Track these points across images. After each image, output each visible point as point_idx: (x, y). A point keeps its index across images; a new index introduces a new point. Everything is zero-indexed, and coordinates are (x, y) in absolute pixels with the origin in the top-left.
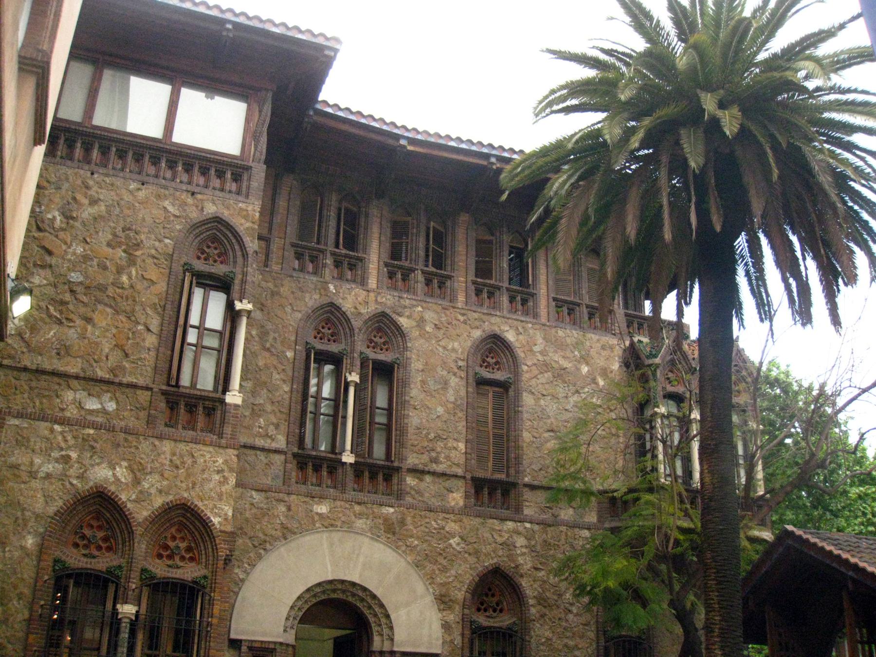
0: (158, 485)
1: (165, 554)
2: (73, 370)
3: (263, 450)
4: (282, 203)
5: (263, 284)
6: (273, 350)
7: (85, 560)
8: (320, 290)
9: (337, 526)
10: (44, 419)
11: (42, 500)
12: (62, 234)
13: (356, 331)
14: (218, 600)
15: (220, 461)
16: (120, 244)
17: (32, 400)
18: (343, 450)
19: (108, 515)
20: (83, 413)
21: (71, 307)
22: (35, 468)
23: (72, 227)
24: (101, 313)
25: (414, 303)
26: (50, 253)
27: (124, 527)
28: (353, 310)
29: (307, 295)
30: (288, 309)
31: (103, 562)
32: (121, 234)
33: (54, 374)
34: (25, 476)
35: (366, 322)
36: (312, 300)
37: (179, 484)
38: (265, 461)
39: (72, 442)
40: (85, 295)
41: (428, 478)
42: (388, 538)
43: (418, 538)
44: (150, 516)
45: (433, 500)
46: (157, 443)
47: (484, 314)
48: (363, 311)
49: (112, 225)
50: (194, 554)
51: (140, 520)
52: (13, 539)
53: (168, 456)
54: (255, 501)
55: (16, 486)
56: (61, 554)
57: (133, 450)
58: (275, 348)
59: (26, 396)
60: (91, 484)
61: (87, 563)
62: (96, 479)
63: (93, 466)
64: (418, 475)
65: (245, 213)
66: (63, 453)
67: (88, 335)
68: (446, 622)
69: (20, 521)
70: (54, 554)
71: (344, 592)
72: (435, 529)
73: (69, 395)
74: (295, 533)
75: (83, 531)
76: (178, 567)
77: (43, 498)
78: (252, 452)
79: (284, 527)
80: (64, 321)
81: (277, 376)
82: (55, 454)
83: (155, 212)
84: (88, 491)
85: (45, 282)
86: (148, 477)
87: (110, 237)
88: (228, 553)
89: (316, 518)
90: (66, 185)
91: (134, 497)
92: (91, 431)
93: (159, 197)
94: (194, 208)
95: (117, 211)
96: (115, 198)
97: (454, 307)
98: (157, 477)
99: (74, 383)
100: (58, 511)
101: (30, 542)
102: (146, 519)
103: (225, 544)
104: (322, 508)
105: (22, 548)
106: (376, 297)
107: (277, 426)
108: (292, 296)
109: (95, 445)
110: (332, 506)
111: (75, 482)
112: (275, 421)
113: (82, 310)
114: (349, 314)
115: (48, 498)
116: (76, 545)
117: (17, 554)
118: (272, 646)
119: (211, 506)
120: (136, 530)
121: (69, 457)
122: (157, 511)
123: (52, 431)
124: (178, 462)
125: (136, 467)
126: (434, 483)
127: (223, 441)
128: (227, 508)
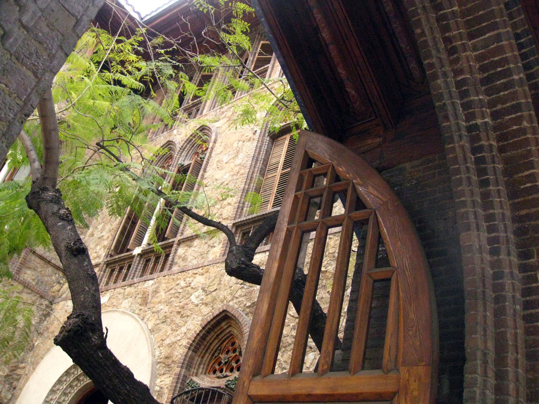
42: (141, 310)
64: (188, 243)
68: (161, 388)
72: (182, 288)
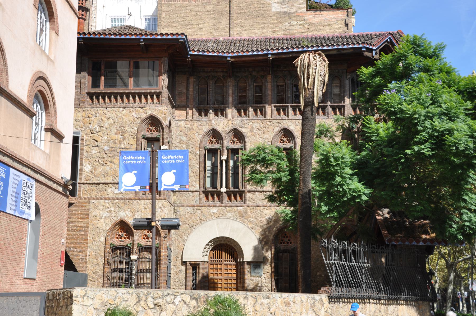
2: (109, 181)
3: (191, 191)
4: (191, 90)
5: (186, 126)
6: (192, 152)
7: (120, 242)
8: (208, 124)
9: (220, 217)
10: (101, 199)
11: (104, 225)
12: (99, 133)
13: (224, 138)
15: (160, 204)
16: (119, 133)
17: (98, 193)
18: (221, 187)
20: (114, 195)
21: (106, 159)
22: (101, 216)
23: (102, 130)
24: (116, 159)
25: (249, 121)
26: (97, 141)
28: (223, 130)
29: (204, 127)
30: (197, 134)
32: (119, 129)
33: (103, 183)
34: (98, 219)
35: (228, 133)
36: (206, 128)
37: (147, 214)
38: (193, 195)
39: (111, 205)
40: (110, 154)
41: (257, 193)
43: (253, 217)
45: (259, 202)
46: (139, 201)
47: (280, 120)
48: (227, 129)
49: (116, 126)
52: (97, 239)
53: (143, 205)
55: (96, 222)
56: (112, 242)
57: (131, 205)
58: (193, 151)
59: (96, 192)
60: (119, 218)
63: (119, 212)
65: (161, 111)
66: (109, 209)
67: (113, 168)
69: (99, 233)
71: (225, 241)
73: (109, 190)
74: (205, 221)
78: (187, 193)
79: (200, 219)
80: (105, 164)
81: (195, 162)
82: (107, 210)
83: (130, 118)
85: (96, 152)
86: (137, 213)
87: (116, 131)
89: (212, 214)
90: (98, 115)
92: (117, 201)
93: (130, 112)
94: (143, 113)
95: (116, 121)
96: (115, 116)
97: (266, 120)
98: (140, 213)
99: (111, 185)
101: (103, 239)
104: (214, 210)
105: (100, 241)
106: (232, 122)
107: (196, 181)
108: (198, 128)
109: (119, 205)
110: (218, 209)
111: (114, 218)
112: (194, 179)
113: (110, 159)
114: (221, 132)
115: (106, 224)
116: (117, 238)
117: (99, 243)
118: (198, 263)
121: (111, 210)
123: (105, 202)
124: (146, 207)
125: (133, 210)
126: (259, 195)
127: (161, 197)
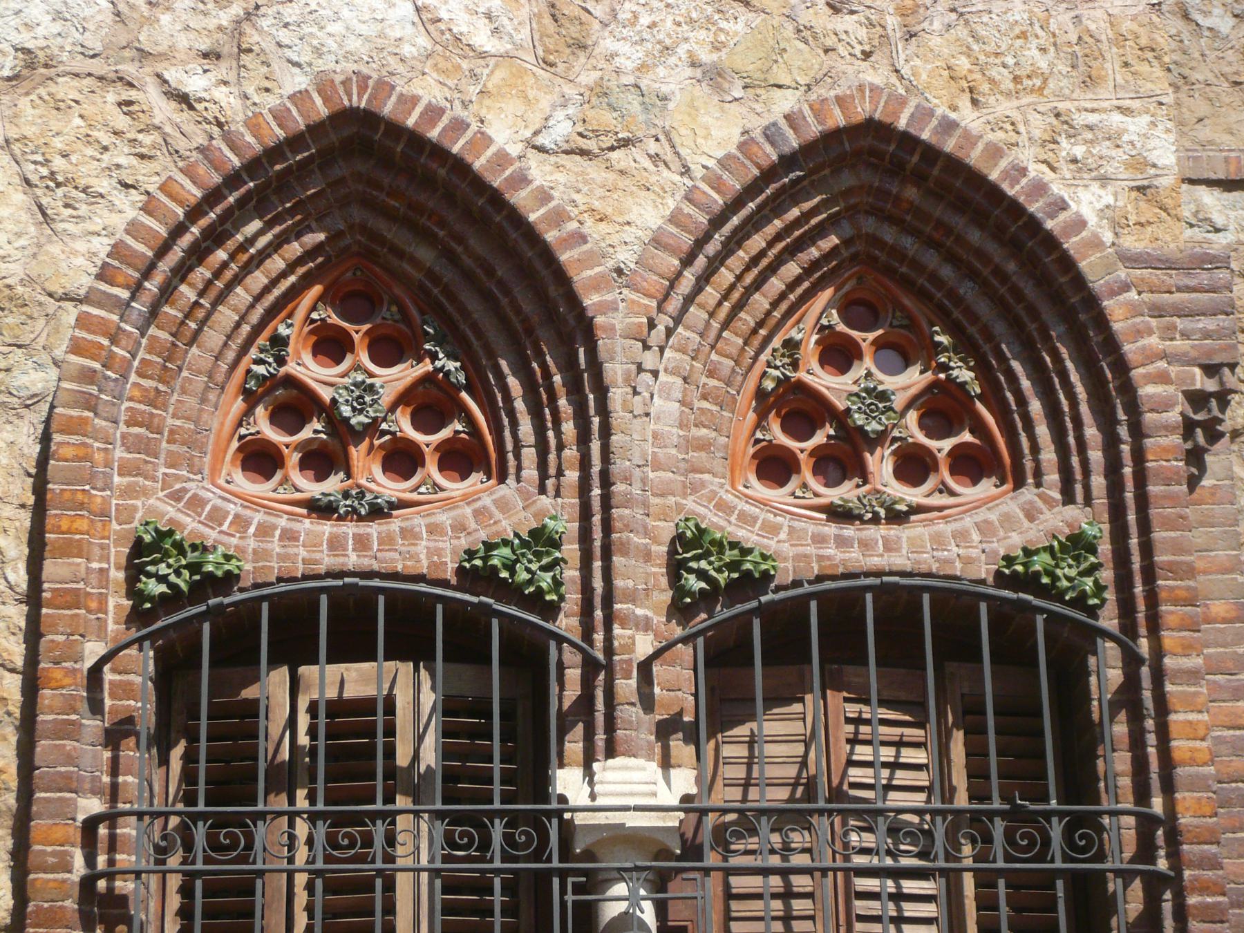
0: (699, 43)
1: (802, 448)
7: (327, 528)
14: (1193, 676)
19: (425, 254)
27: (527, 307)
31: (433, 530)
44: (675, 218)
50: (979, 428)
51: (626, 257)
54: (1222, 240)
60: (299, 81)
61: (336, 544)
62: (318, 52)
70: (126, 515)
75: (291, 368)
76: (897, 517)
77: (19, 197)
84: (280, 116)
88: (1201, 381)
91: (561, 130)
100: (117, 250)
102: (657, 241)
103: (1168, 333)
111: (195, 83)
119: (1038, 125)
120: (612, 307)
122: (717, 185)
128: (1135, 126)
